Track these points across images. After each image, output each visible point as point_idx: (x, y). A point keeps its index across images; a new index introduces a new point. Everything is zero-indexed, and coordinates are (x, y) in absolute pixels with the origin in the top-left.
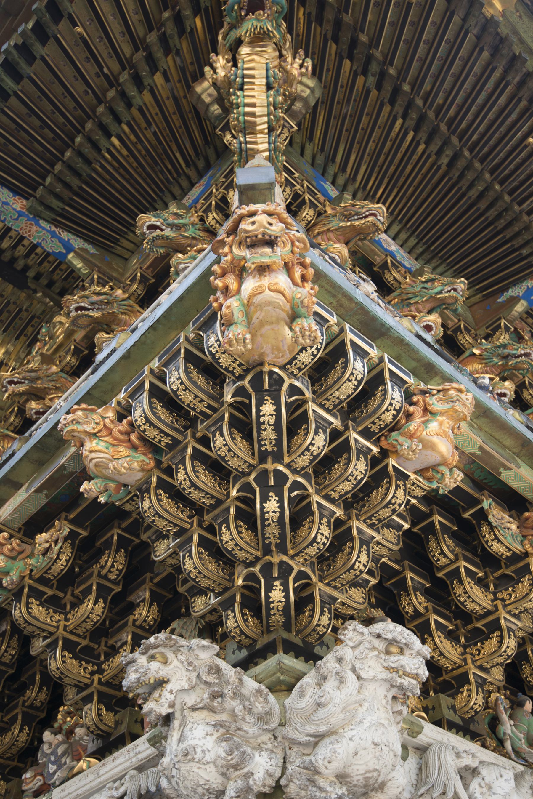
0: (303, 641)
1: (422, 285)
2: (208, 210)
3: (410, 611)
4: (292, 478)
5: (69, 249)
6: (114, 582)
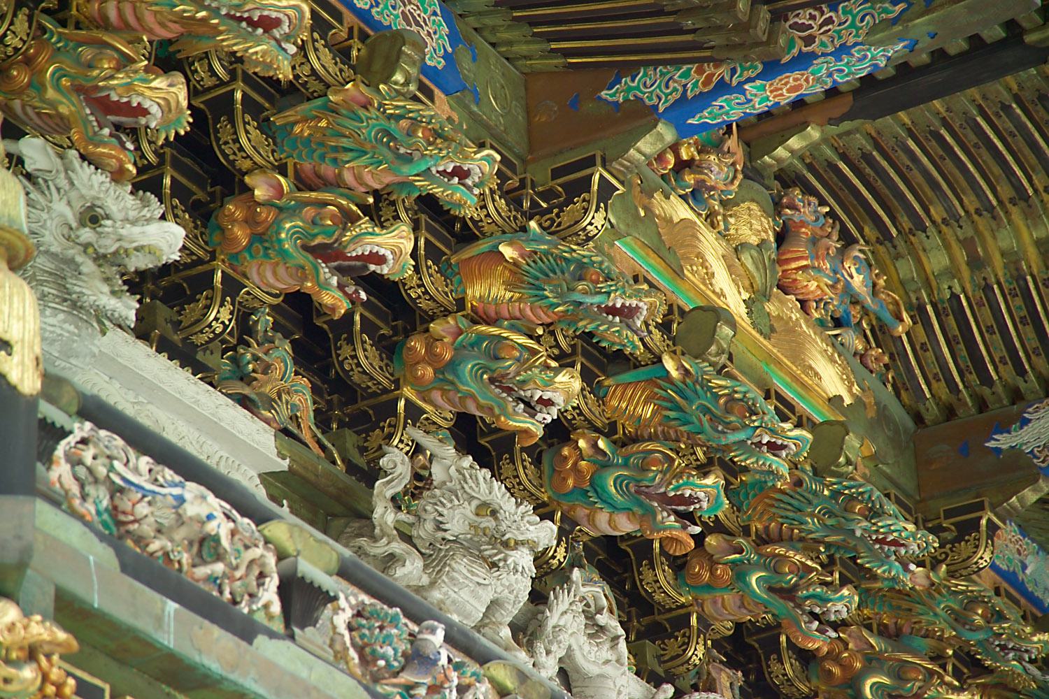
1: (384, 123)
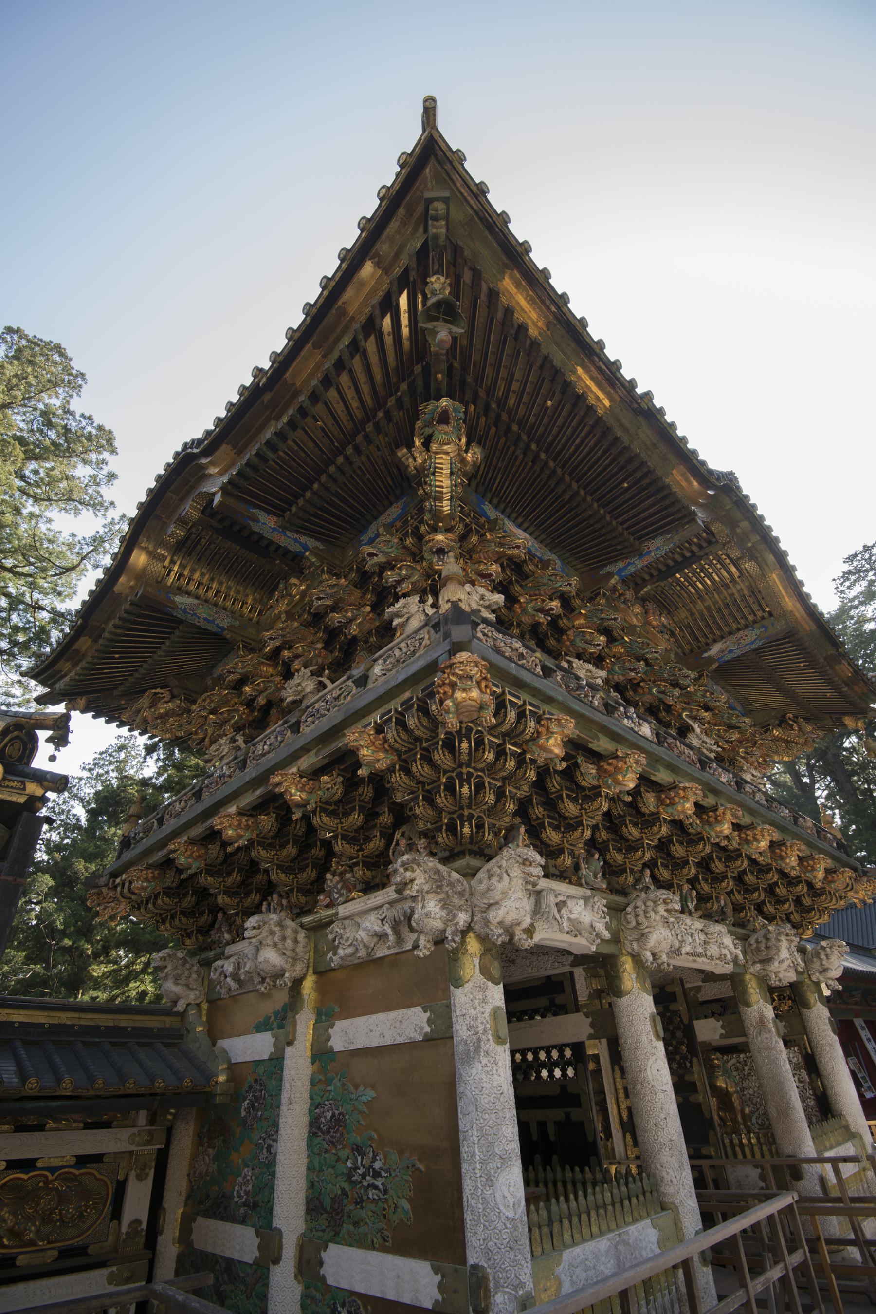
0: (479, 848)
2: (406, 535)
3: (535, 817)
4: (475, 774)
5: (306, 548)
6: (368, 803)
